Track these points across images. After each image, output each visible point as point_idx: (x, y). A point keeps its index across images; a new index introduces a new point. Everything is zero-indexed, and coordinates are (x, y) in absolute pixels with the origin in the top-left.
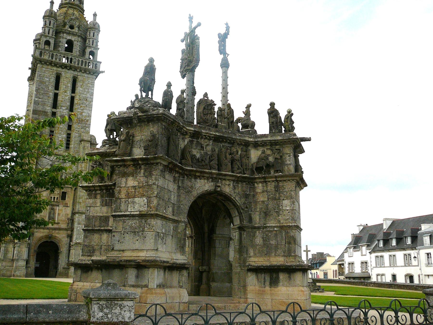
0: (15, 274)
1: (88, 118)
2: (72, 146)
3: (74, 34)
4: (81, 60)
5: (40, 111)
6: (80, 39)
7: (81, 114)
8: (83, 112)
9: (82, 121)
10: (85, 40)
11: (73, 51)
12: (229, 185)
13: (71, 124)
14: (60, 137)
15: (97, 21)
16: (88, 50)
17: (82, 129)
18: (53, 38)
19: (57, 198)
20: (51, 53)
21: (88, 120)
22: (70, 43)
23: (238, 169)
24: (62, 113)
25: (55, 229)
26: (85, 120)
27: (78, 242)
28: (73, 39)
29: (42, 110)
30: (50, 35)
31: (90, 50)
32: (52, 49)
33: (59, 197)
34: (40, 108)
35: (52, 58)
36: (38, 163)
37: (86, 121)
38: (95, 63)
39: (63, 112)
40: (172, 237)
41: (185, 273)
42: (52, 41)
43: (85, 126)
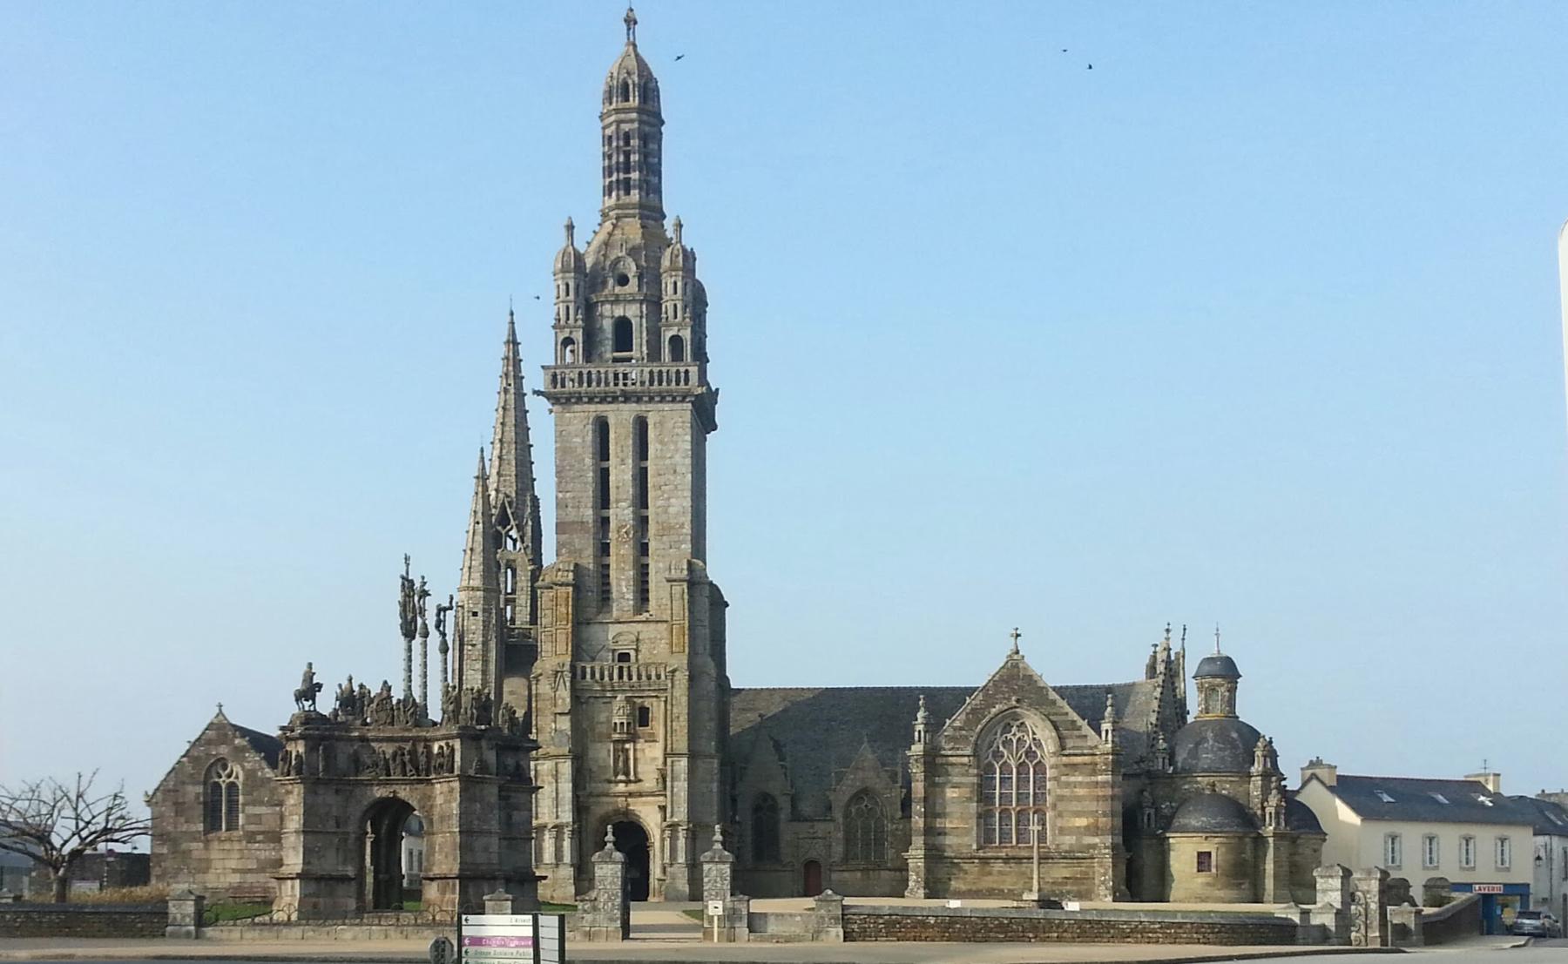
0: (555, 895)
1: (682, 519)
2: (651, 595)
5: (573, 523)
7: (666, 512)
8: (669, 506)
9: (671, 528)
12: (405, 789)
13: (646, 541)
14: (623, 577)
17: (671, 548)
19: (629, 724)
21: (683, 524)
23: (411, 771)
24: (623, 518)
25: (631, 795)
26: (677, 524)
27: (676, 820)
29: (576, 519)
33: (632, 721)
34: (572, 515)
36: (582, 649)
37: (680, 527)
39: (623, 515)
40: (338, 849)
41: (353, 883)
43: (676, 539)
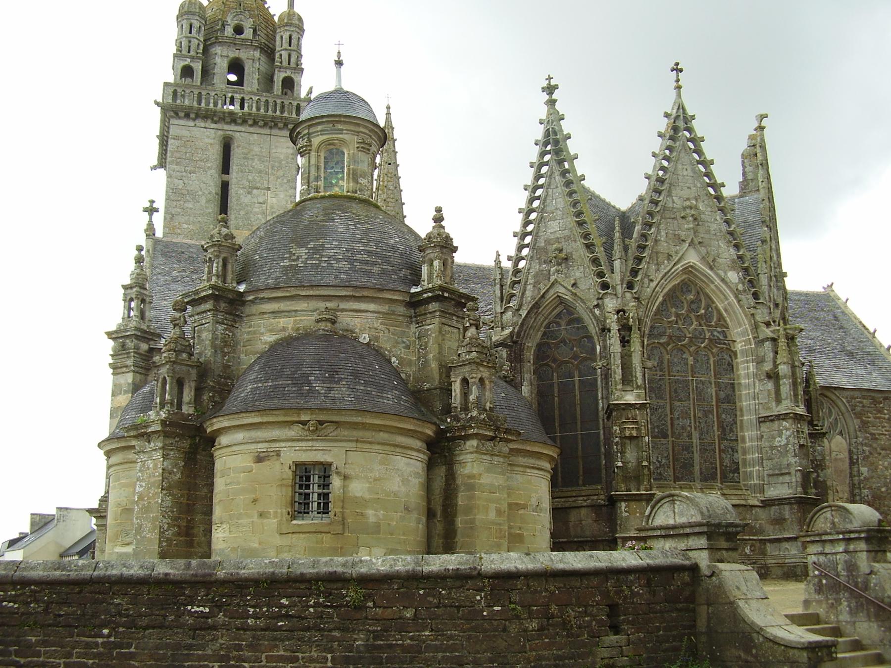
3: (244, 44)
4: (263, 99)
6: (257, 54)
10: (269, 52)
11: (245, 85)
15: (297, 9)
16: (279, 77)
18: (198, 58)
20: (196, 92)
22: (236, 67)
28: (243, 54)
30: (192, 53)
31: (283, 75)
32: (199, 84)
35: (199, 103)
38: (295, 103)
42: (197, 67)
